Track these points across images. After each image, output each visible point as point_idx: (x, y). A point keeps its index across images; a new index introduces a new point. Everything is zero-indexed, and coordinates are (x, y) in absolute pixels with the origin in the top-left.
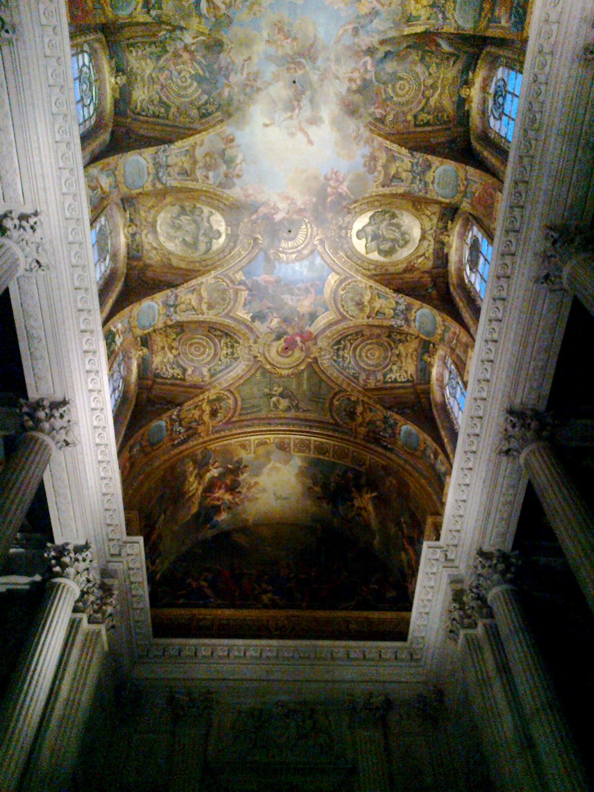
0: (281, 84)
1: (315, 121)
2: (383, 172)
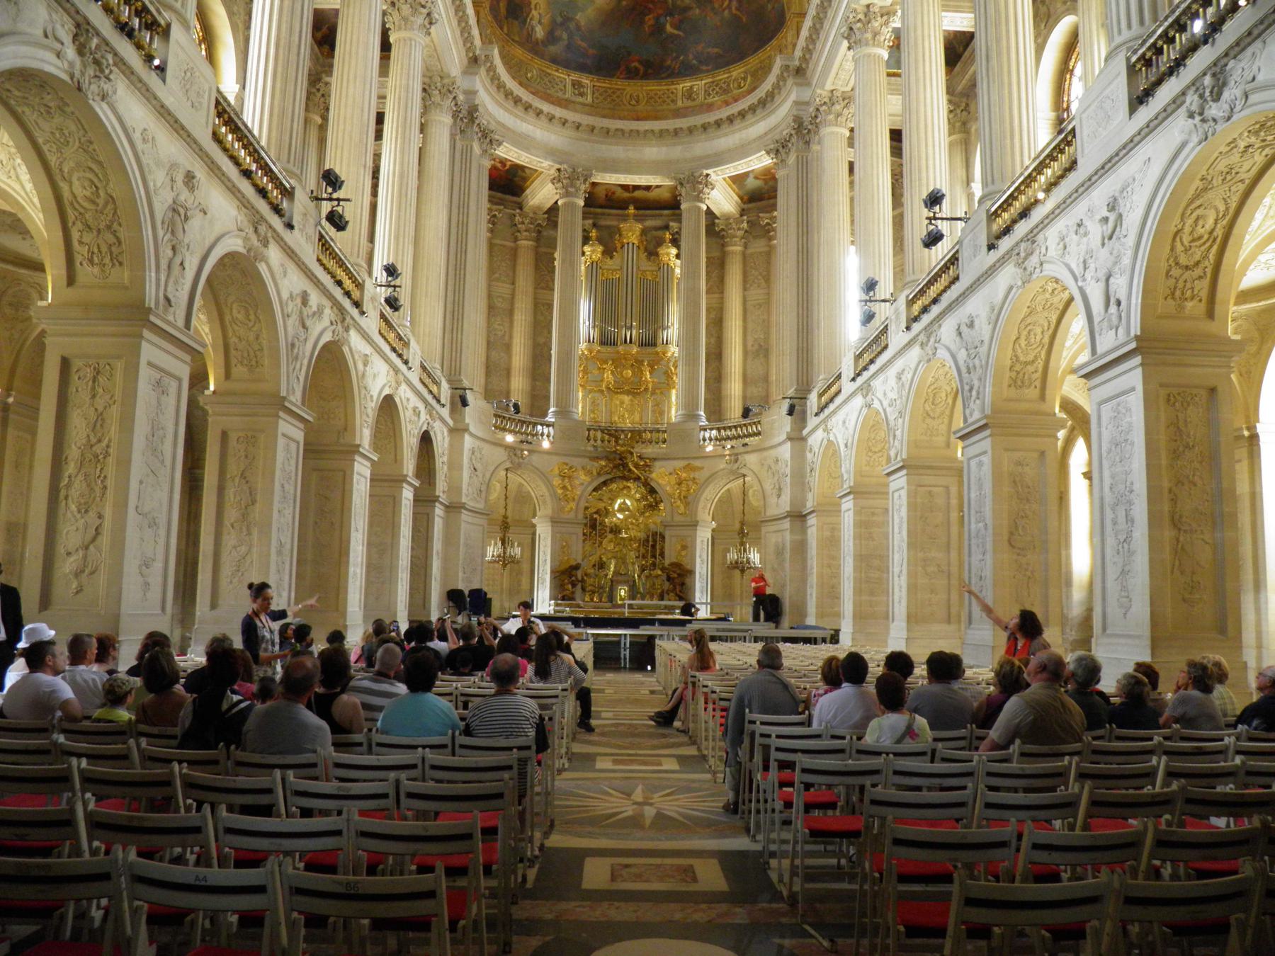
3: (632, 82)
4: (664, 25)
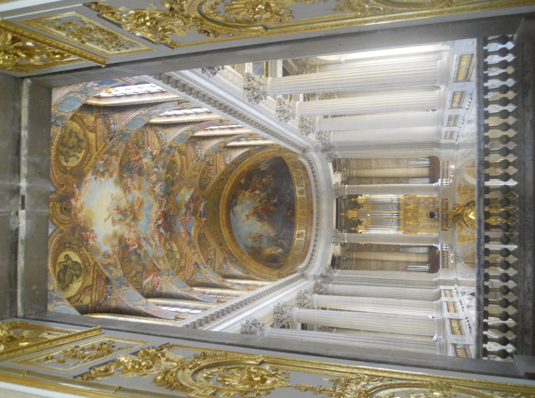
0: (126, 204)
1: (113, 222)
2: (106, 263)
3: (296, 215)
4: (275, 203)
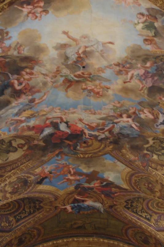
1: (64, 46)
